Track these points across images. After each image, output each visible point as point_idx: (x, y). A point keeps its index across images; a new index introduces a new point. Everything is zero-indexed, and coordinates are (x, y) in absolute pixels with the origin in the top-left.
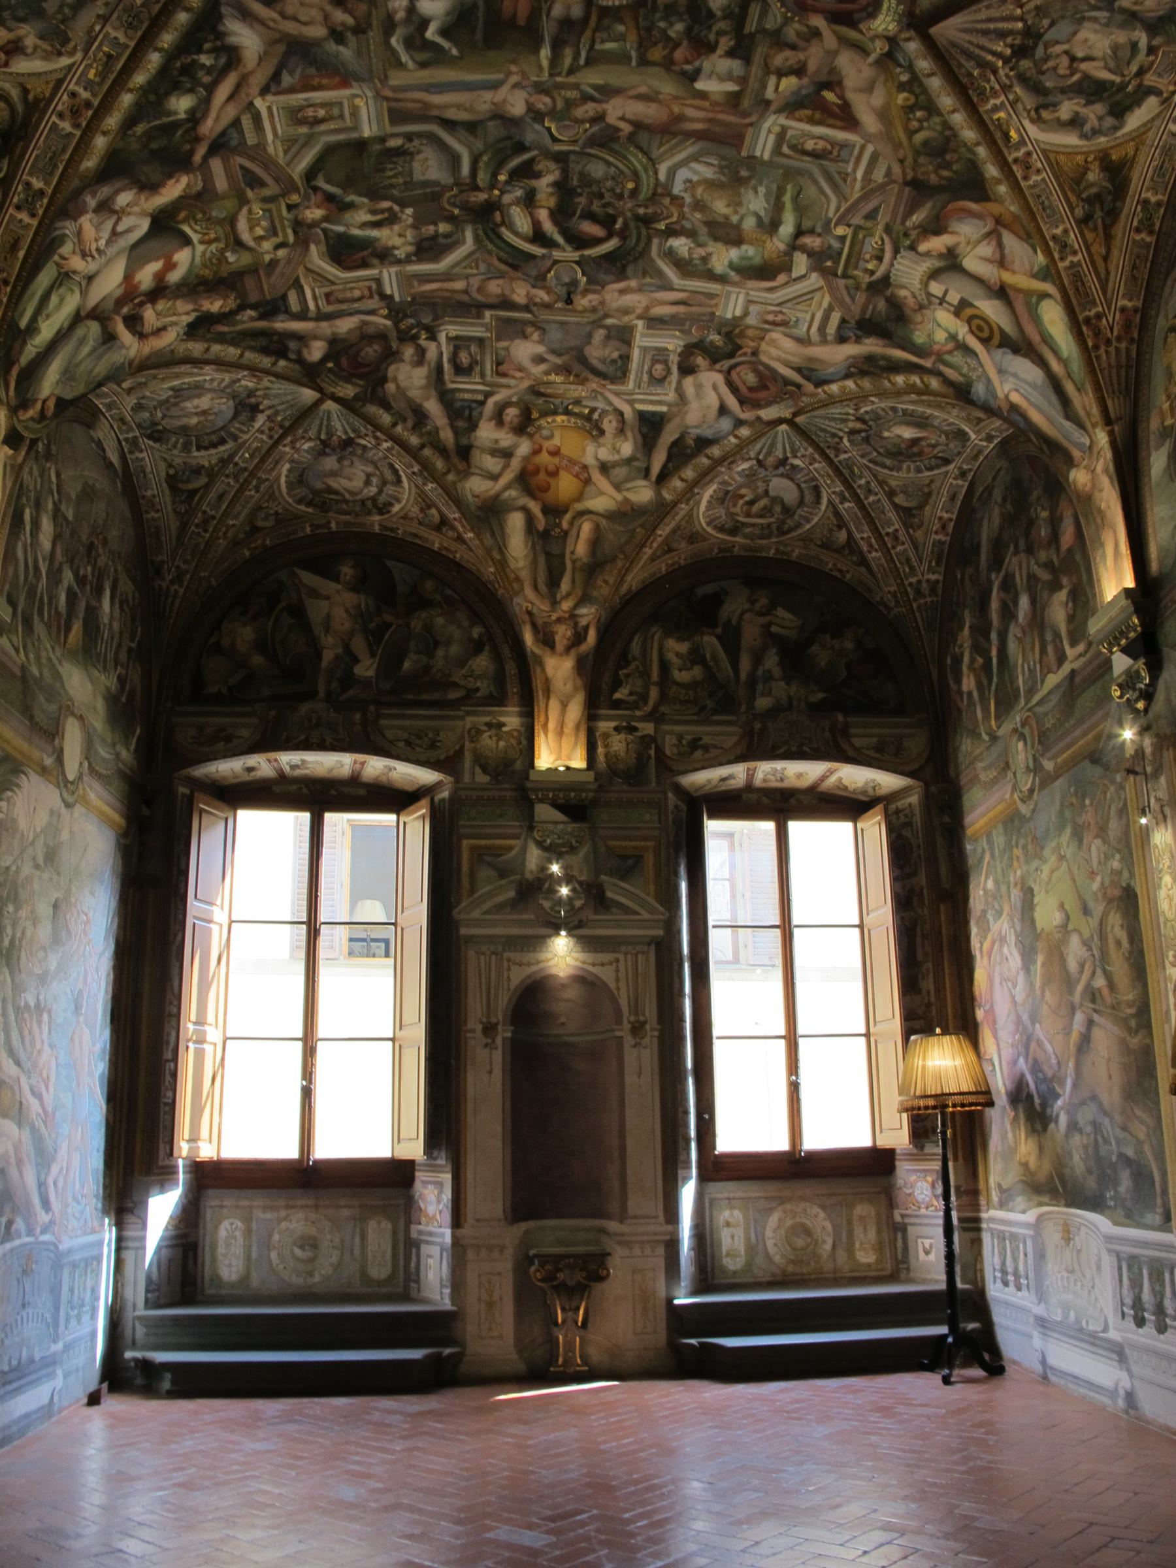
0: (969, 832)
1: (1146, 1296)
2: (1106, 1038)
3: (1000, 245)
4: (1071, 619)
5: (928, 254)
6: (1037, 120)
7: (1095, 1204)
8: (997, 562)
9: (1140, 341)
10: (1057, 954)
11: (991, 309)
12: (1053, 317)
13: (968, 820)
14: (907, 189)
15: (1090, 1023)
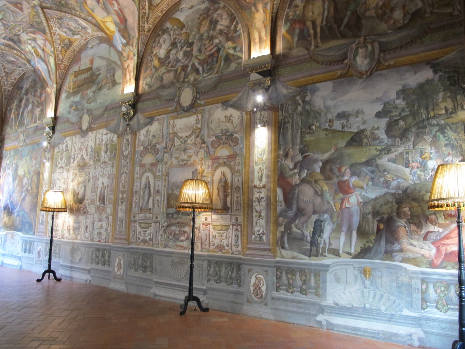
0: (5, 149)
1: (28, 247)
2: (28, 199)
3: (45, 42)
4: (40, 115)
5: (30, 36)
6: (59, 28)
7: (20, 230)
8: (26, 94)
9: (67, 71)
10: (21, 180)
11: (40, 51)
12: (52, 60)
13: (5, 146)
14: (29, 25)
15: (26, 196)
